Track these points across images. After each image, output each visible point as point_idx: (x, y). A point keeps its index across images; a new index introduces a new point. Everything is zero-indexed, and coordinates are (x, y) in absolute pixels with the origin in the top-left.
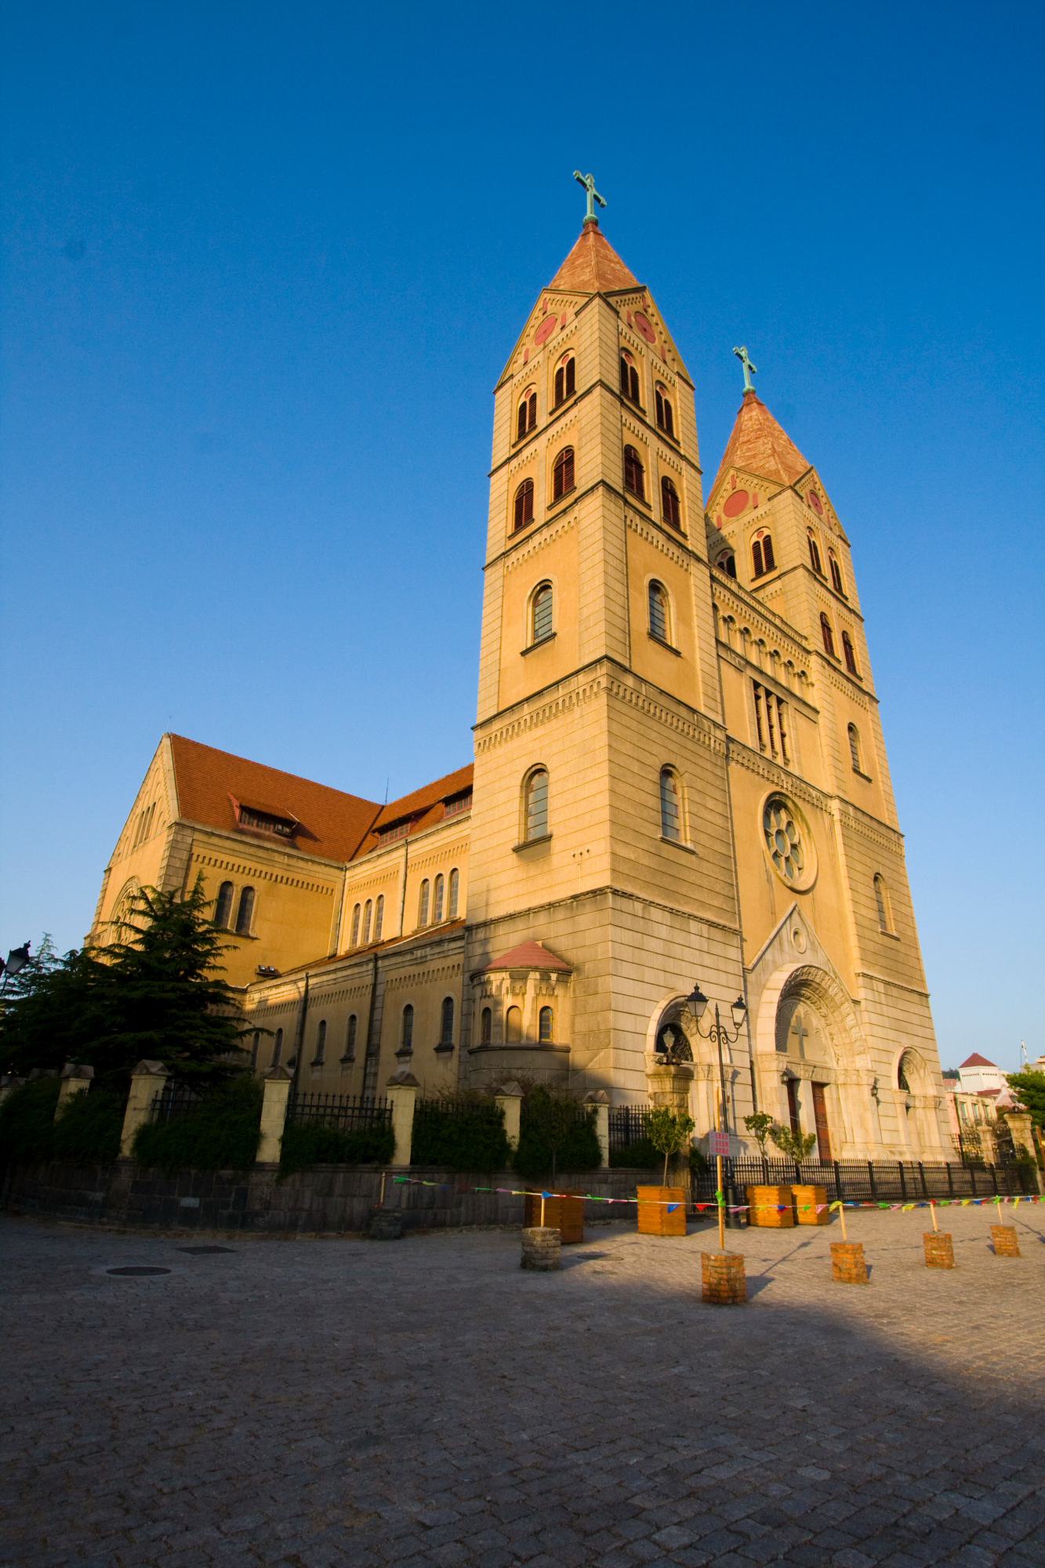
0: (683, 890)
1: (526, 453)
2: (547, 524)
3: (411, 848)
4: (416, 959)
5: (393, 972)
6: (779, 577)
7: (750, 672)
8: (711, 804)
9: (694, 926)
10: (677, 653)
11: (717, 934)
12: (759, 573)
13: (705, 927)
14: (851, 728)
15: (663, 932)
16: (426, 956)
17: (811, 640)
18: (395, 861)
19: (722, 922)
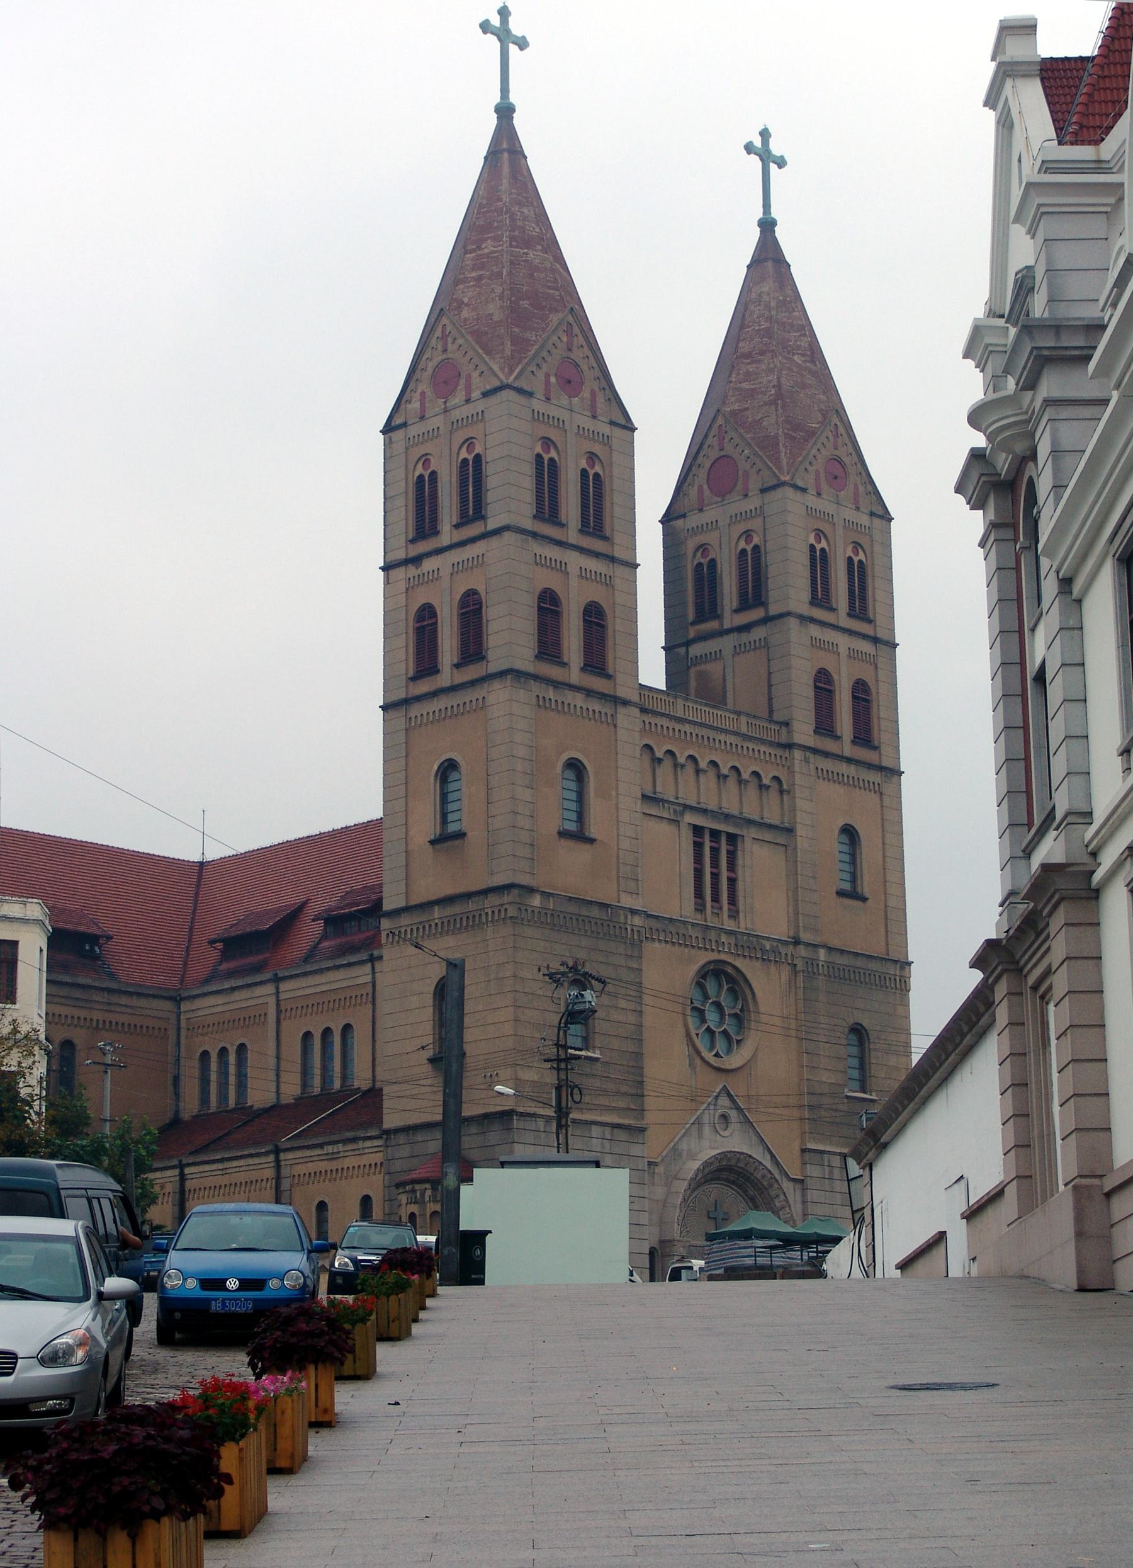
1: (428, 565)
2: (453, 689)
3: (284, 986)
4: (327, 1154)
5: (300, 1166)
6: (766, 620)
7: (690, 818)
8: (622, 1004)
9: (596, 1131)
10: (592, 841)
11: (622, 1135)
12: (744, 605)
13: (608, 1130)
14: (849, 832)
16: (339, 1152)
17: (796, 726)
18: (260, 1001)
19: (626, 1122)
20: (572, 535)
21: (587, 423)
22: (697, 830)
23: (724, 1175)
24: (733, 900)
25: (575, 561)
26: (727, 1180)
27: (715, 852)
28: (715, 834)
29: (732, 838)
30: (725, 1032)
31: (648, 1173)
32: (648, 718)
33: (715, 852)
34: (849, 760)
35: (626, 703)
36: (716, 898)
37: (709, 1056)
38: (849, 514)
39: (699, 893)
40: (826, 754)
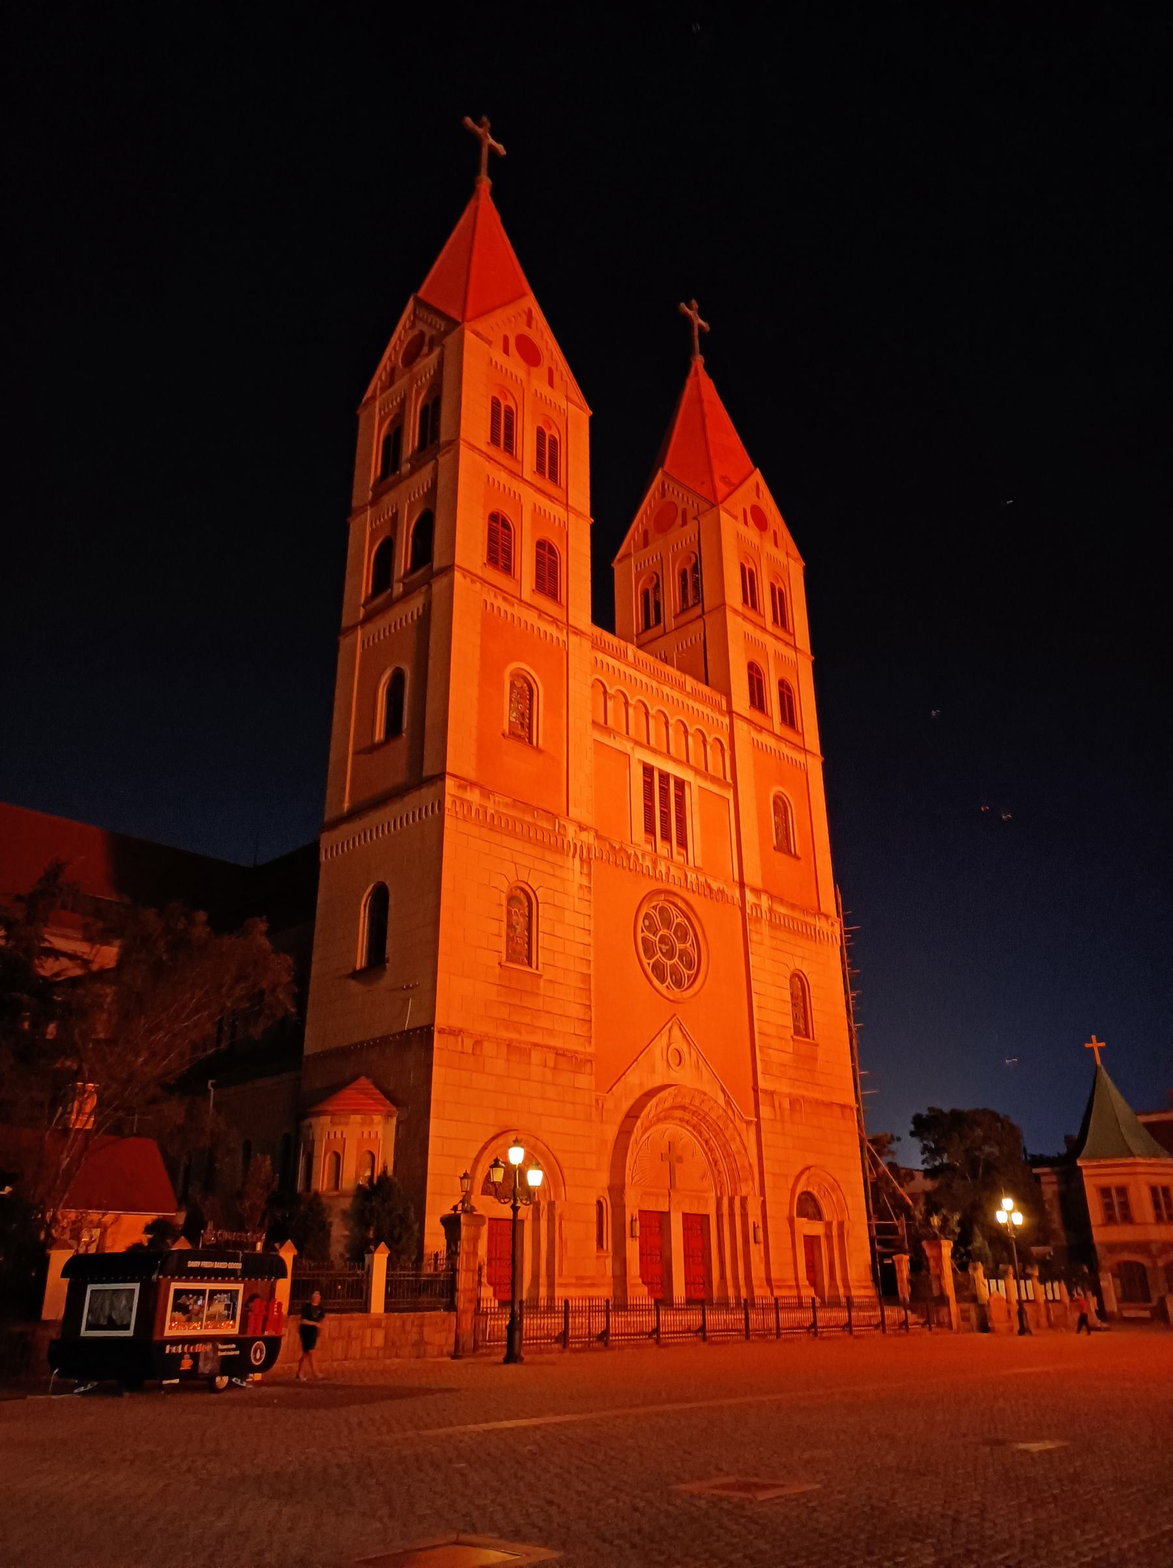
0: (527, 1020)
15: (500, 1066)
20: (528, 474)
21: (545, 390)
22: (648, 770)
23: (679, 1113)
24: (683, 843)
25: (529, 497)
26: (681, 1120)
27: (664, 791)
28: (665, 777)
29: (680, 784)
30: (674, 966)
31: (597, 1109)
32: (600, 656)
33: (664, 791)
34: (779, 738)
35: (578, 632)
36: (666, 837)
37: (662, 988)
38: (769, 547)
39: (649, 829)
40: (760, 729)
